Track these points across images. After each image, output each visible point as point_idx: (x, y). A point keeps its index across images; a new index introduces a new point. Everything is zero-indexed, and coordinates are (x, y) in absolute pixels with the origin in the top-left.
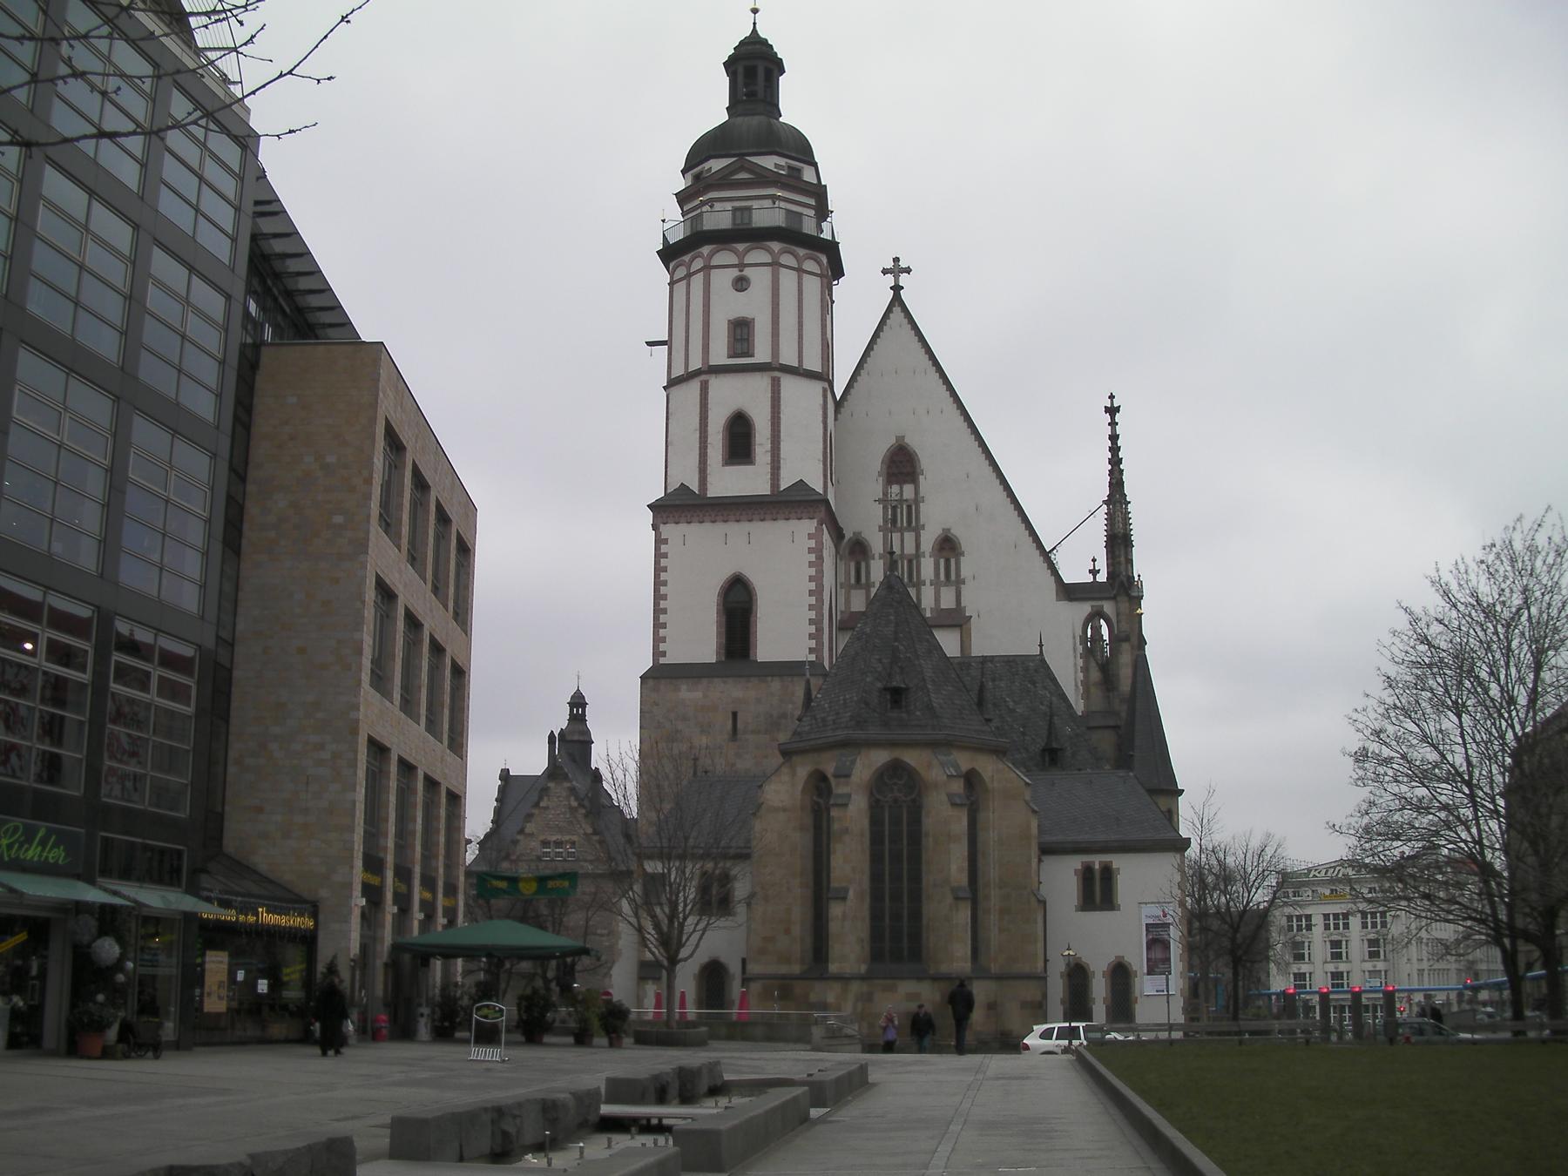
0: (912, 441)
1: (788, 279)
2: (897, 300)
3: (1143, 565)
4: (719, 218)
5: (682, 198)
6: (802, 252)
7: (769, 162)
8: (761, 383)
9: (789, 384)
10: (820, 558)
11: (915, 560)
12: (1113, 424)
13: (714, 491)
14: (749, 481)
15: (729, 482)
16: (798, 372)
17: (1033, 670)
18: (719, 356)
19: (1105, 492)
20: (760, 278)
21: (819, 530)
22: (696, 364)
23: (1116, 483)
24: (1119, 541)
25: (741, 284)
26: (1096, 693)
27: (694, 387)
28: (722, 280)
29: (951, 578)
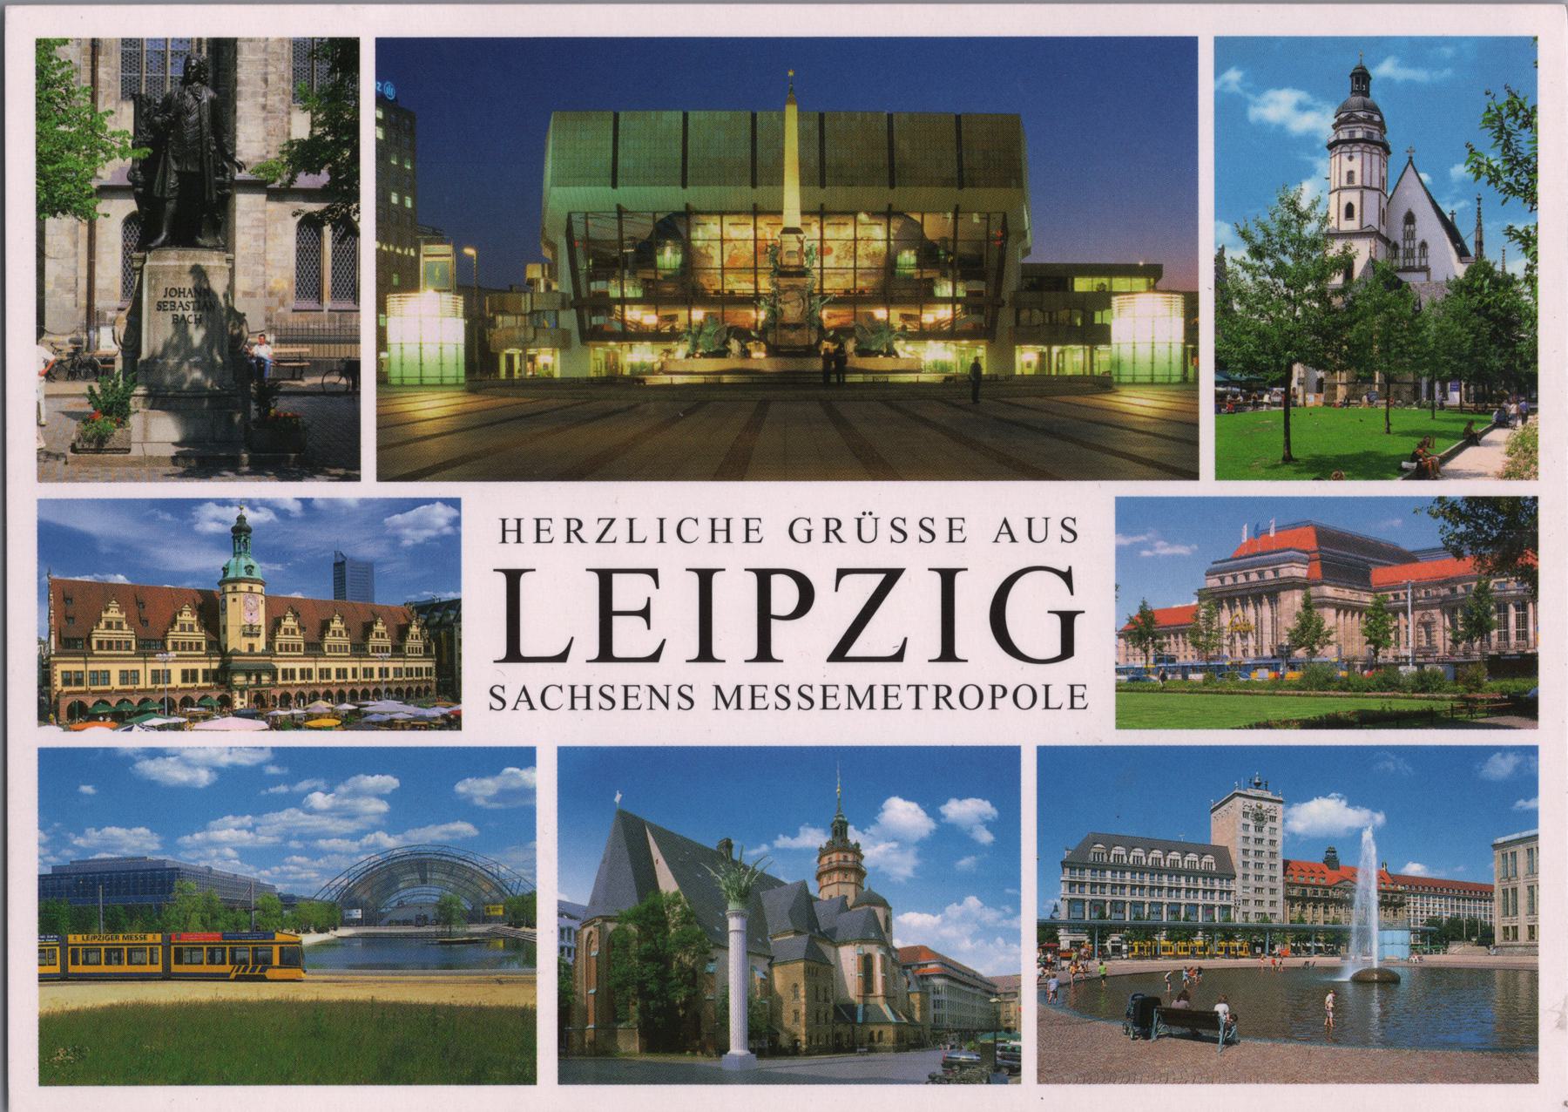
0: (1414, 211)
1: (1367, 156)
2: (1410, 161)
4: (1344, 135)
5: (1335, 126)
7: (1361, 115)
9: (1366, 192)
11: (1413, 250)
14: (1353, 225)
18: (1344, 183)
22: (1337, 186)
23: (1479, 224)
25: (1351, 158)
27: (1336, 194)
28: (1345, 158)
29: (1424, 254)
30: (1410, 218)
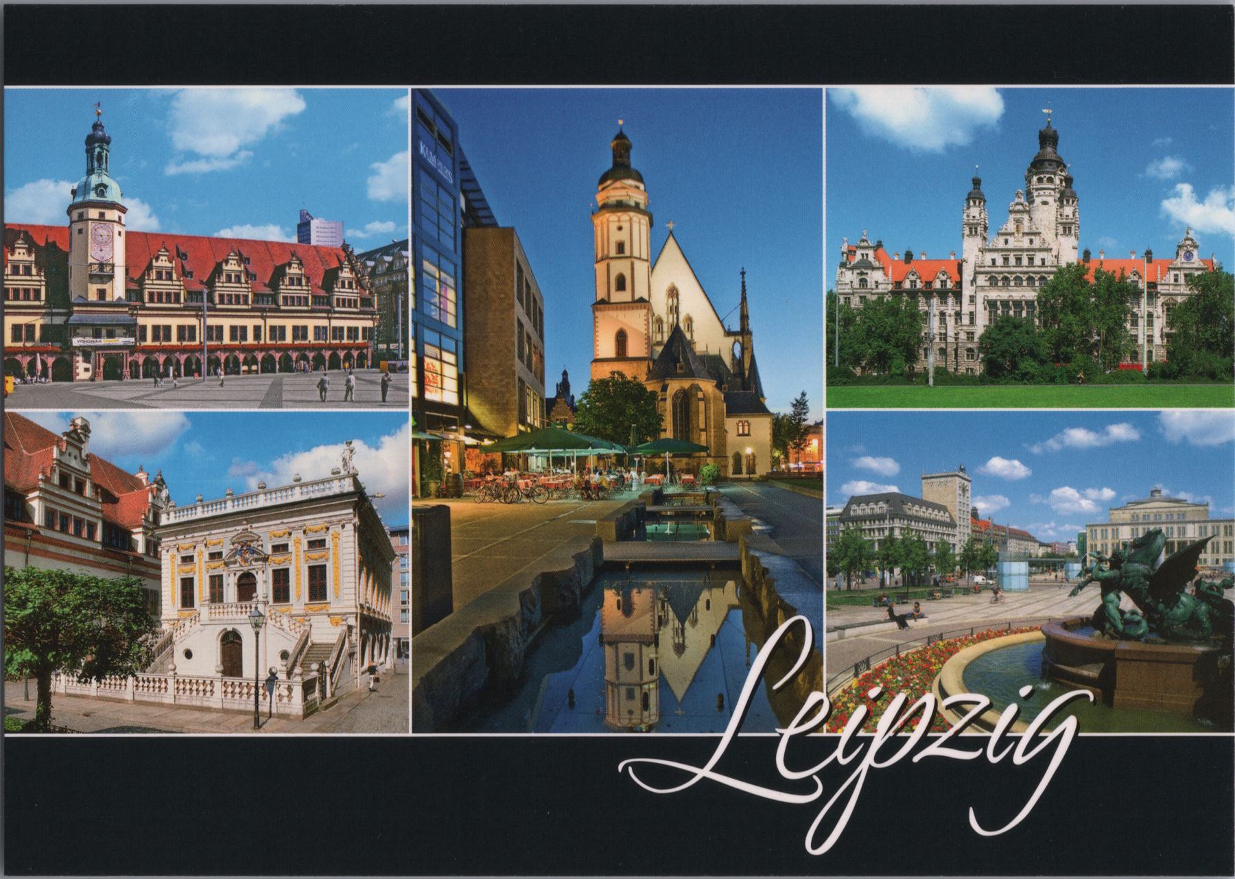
3: (752, 325)
6: (640, 216)
8: (627, 263)
10: (648, 322)
12: (743, 277)
13: (613, 300)
14: (625, 296)
15: (617, 297)
16: (640, 259)
17: (717, 359)
18: (613, 253)
19: (740, 301)
20: (626, 226)
21: (648, 313)
24: (744, 318)
25: (620, 228)
26: (737, 368)
30: (673, 292)
